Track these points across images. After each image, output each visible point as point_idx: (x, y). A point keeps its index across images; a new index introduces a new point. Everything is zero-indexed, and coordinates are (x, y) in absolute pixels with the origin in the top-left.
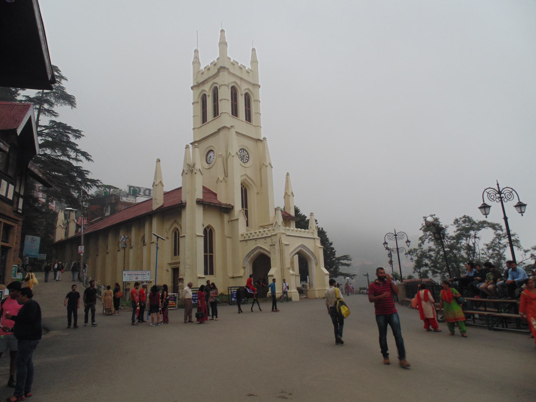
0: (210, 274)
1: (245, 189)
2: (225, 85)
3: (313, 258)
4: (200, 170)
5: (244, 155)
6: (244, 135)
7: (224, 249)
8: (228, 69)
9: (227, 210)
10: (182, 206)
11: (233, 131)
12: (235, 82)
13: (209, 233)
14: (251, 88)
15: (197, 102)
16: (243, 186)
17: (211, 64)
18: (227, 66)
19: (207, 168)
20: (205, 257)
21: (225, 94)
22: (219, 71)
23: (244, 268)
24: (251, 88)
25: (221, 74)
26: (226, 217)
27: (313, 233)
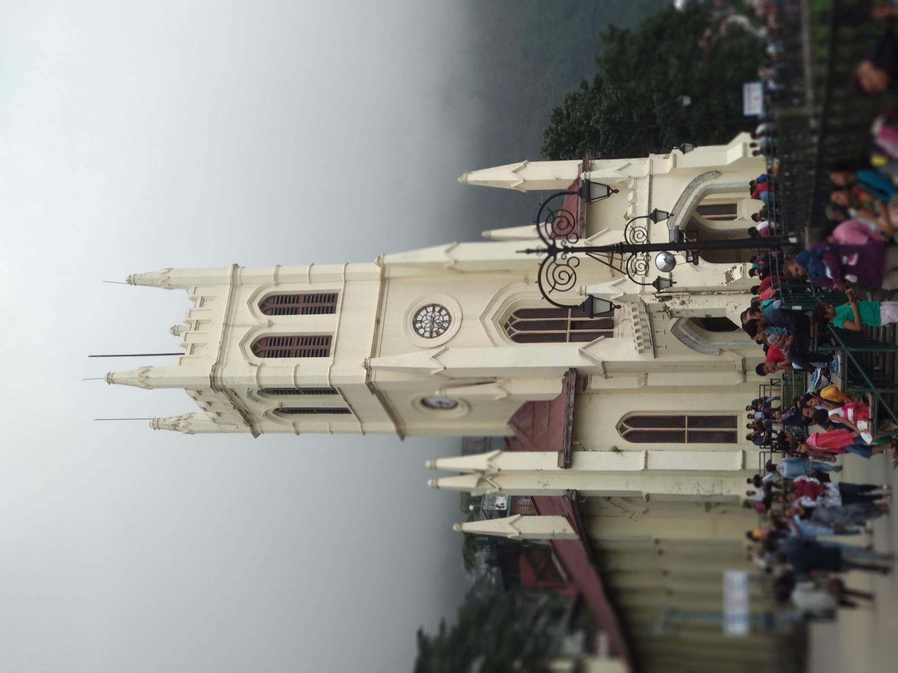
0: (735, 426)
2: (258, 377)
3: (702, 186)
4: (490, 459)
5: (432, 322)
6: (378, 322)
8: (214, 370)
9: (577, 381)
11: (374, 363)
12: (242, 344)
14: (245, 294)
15: (294, 425)
16: (511, 320)
18: (208, 372)
19: (466, 410)
20: (695, 438)
22: (222, 389)
23: (721, 351)
24: (245, 294)
25: (228, 384)
26: (597, 383)
27: (636, 179)
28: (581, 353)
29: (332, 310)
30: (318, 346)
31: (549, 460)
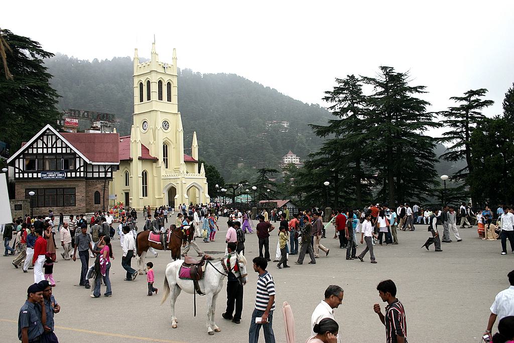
1: (166, 146)
5: (166, 125)
7: (153, 184)
9: (155, 160)
10: (131, 160)
13: (145, 174)
21: (154, 88)
30: (160, 98)
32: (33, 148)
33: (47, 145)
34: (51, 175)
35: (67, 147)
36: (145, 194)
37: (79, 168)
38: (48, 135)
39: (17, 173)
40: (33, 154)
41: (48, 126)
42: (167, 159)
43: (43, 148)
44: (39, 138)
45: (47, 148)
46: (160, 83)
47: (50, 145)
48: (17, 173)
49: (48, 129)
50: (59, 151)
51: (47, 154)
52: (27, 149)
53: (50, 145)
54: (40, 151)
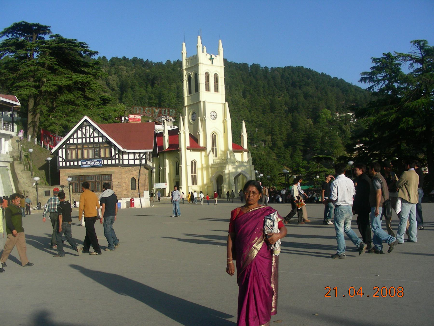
9: (204, 149)
11: (206, 103)
13: (193, 164)
17: (193, 57)
20: (192, 176)
26: (203, 153)
28: (210, 151)
29: (215, 91)
30: (208, 88)
31: (188, 145)
32: (73, 139)
33: (85, 135)
34: (90, 163)
35: (103, 136)
36: (194, 181)
37: (115, 156)
38: (86, 126)
39: (61, 162)
40: (73, 144)
41: (86, 118)
42: (216, 148)
43: (82, 138)
44: (78, 129)
45: (86, 138)
46: (207, 75)
47: (88, 135)
48: (61, 162)
49: (86, 121)
50: (96, 140)
51: (86, 143)
52: (68, 139)
53: (88, 135)
54: (80, 141)
